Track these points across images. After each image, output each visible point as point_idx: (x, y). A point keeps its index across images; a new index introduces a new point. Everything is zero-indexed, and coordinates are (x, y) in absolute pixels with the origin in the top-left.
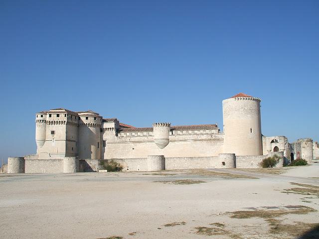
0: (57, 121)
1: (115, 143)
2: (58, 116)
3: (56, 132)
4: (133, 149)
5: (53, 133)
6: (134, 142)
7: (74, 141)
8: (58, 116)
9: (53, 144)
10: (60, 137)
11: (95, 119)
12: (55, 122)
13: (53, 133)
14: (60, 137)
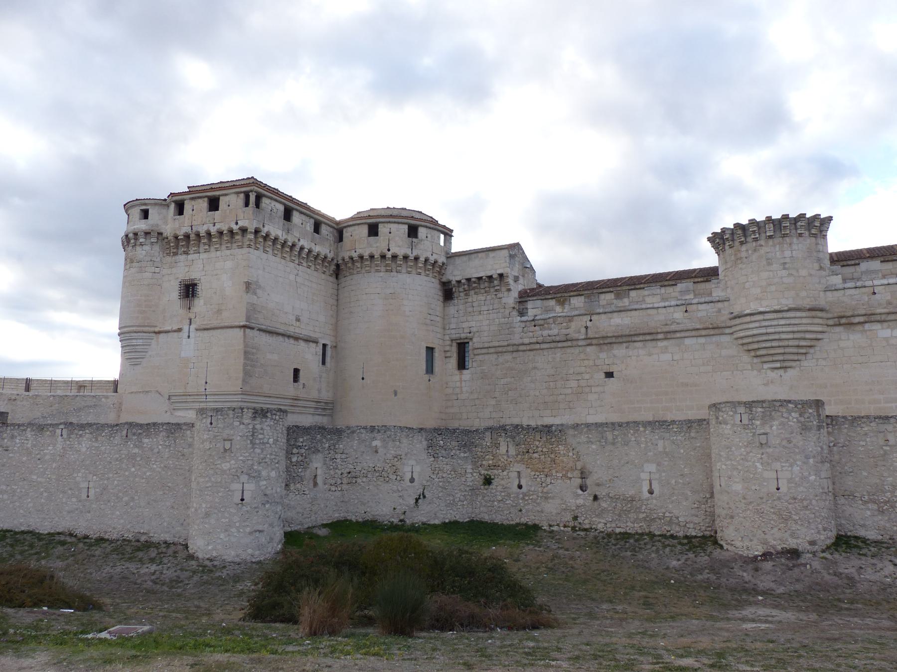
0: (209, 234)
1: (516, 349)
2: (214, 204)
3: (201, 290)
4: (610, 375)
5: (189, 290)
6: (606, 342)
7: (307, 340)
8: (214, 204)
9: (188, 346)
10: (219, 311)
12: (198, 235)
13: (189, 290)
14: (219, 311)
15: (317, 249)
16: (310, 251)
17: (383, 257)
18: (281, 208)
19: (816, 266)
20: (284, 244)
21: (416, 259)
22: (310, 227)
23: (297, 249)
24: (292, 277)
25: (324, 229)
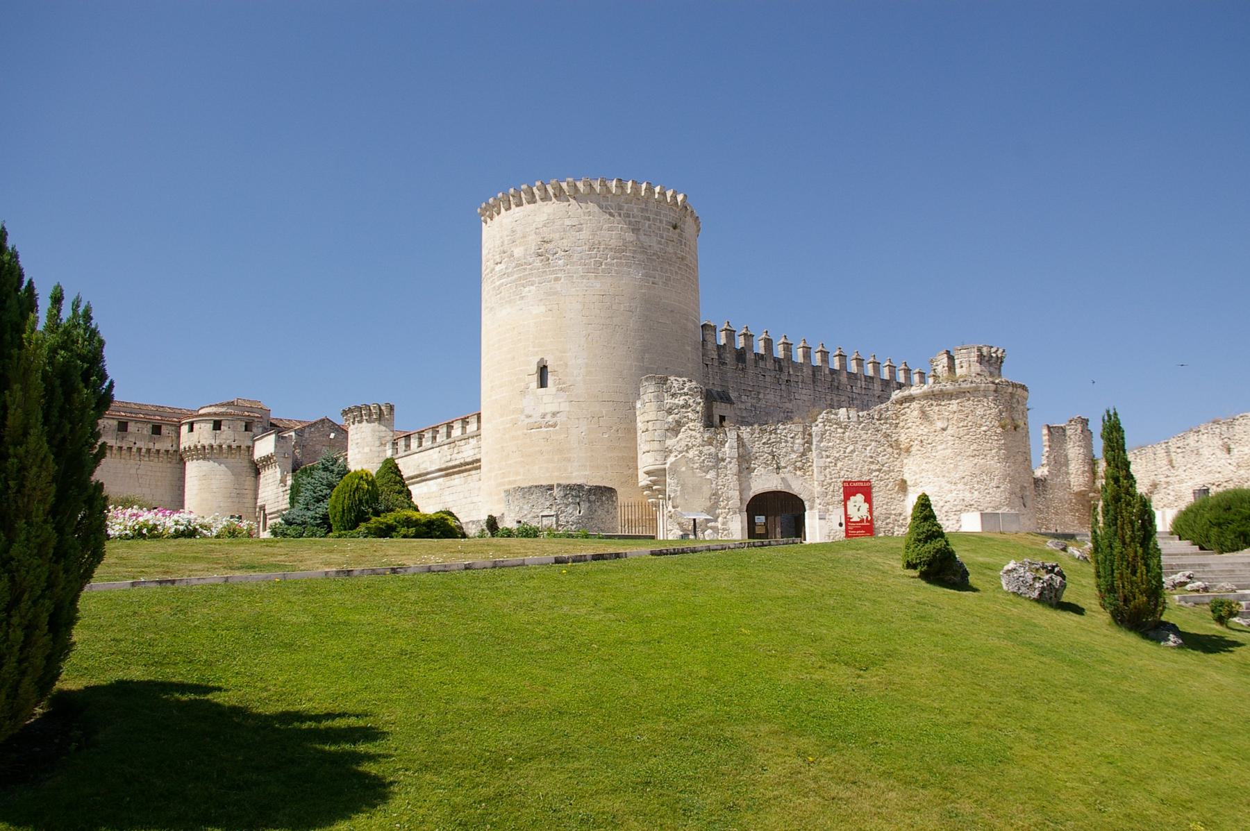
11: (217, 426)
15: (157, 446)
16: (149, 450)
17: (196, 446)
18: (115, 423)
19: (377, 443)
20: (120, 448)
21: (221, 446)
22: (147, 430)
23: (134, 450)
24: (133, 471)
25: (164, 430)
